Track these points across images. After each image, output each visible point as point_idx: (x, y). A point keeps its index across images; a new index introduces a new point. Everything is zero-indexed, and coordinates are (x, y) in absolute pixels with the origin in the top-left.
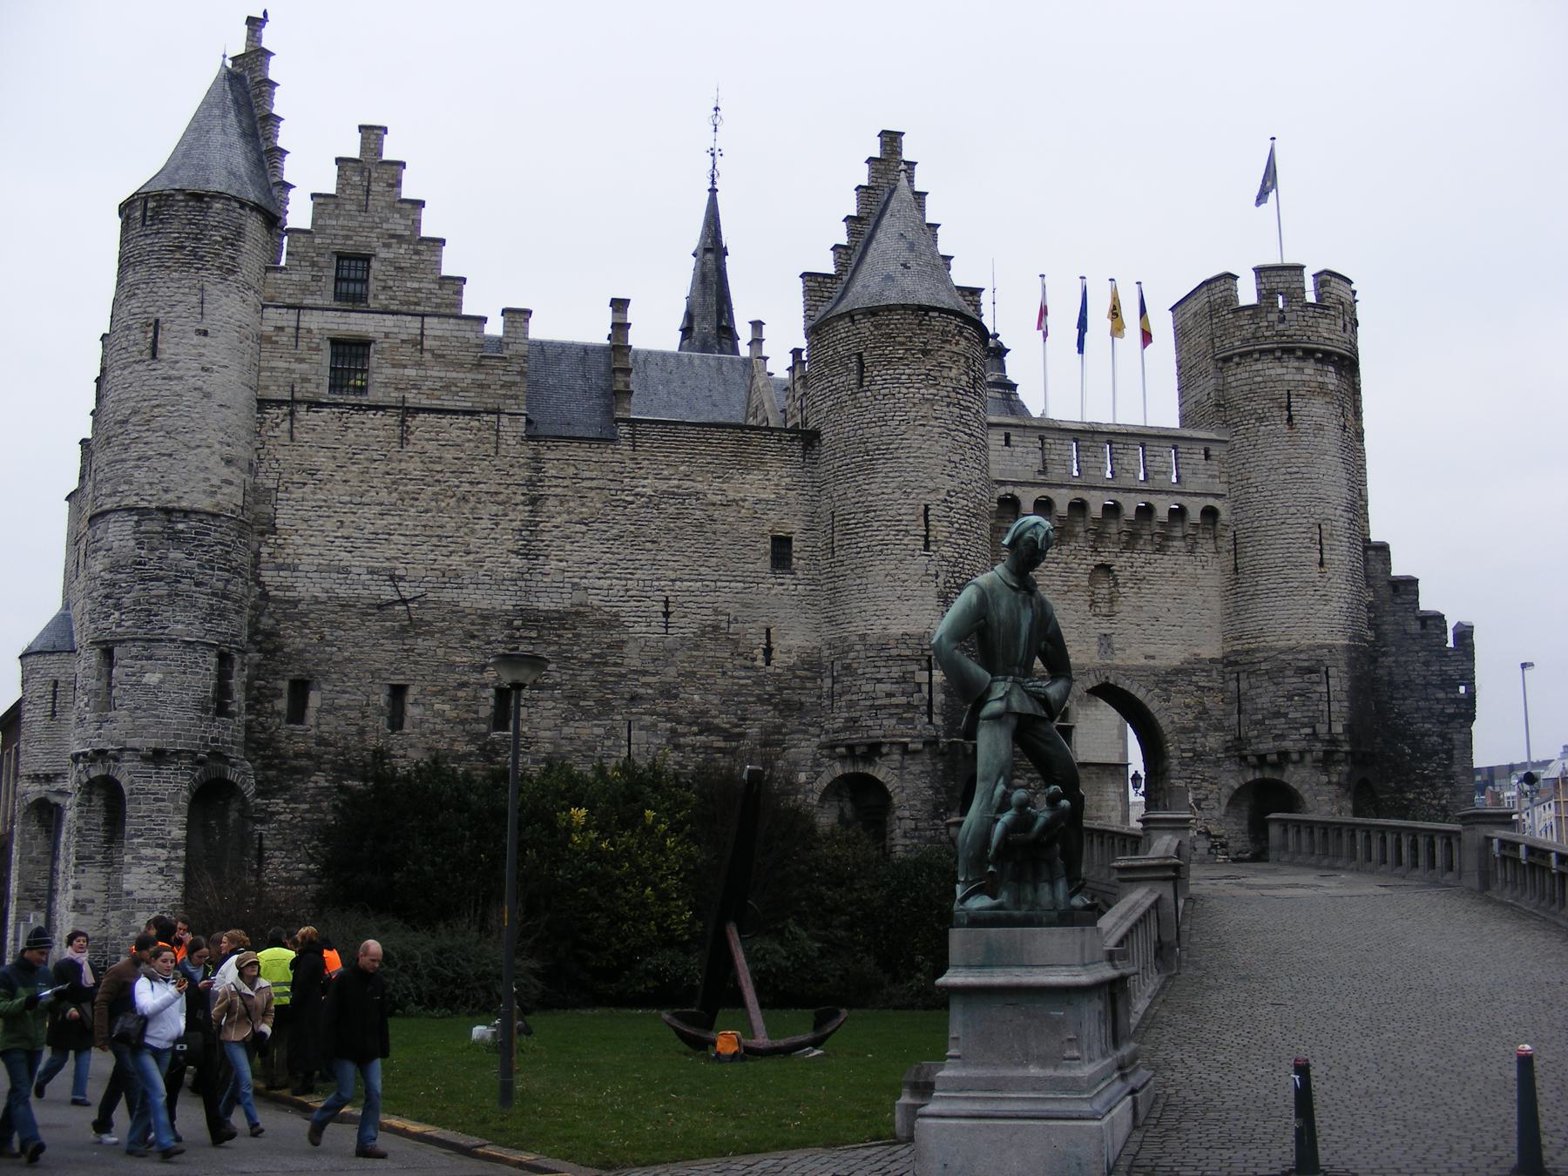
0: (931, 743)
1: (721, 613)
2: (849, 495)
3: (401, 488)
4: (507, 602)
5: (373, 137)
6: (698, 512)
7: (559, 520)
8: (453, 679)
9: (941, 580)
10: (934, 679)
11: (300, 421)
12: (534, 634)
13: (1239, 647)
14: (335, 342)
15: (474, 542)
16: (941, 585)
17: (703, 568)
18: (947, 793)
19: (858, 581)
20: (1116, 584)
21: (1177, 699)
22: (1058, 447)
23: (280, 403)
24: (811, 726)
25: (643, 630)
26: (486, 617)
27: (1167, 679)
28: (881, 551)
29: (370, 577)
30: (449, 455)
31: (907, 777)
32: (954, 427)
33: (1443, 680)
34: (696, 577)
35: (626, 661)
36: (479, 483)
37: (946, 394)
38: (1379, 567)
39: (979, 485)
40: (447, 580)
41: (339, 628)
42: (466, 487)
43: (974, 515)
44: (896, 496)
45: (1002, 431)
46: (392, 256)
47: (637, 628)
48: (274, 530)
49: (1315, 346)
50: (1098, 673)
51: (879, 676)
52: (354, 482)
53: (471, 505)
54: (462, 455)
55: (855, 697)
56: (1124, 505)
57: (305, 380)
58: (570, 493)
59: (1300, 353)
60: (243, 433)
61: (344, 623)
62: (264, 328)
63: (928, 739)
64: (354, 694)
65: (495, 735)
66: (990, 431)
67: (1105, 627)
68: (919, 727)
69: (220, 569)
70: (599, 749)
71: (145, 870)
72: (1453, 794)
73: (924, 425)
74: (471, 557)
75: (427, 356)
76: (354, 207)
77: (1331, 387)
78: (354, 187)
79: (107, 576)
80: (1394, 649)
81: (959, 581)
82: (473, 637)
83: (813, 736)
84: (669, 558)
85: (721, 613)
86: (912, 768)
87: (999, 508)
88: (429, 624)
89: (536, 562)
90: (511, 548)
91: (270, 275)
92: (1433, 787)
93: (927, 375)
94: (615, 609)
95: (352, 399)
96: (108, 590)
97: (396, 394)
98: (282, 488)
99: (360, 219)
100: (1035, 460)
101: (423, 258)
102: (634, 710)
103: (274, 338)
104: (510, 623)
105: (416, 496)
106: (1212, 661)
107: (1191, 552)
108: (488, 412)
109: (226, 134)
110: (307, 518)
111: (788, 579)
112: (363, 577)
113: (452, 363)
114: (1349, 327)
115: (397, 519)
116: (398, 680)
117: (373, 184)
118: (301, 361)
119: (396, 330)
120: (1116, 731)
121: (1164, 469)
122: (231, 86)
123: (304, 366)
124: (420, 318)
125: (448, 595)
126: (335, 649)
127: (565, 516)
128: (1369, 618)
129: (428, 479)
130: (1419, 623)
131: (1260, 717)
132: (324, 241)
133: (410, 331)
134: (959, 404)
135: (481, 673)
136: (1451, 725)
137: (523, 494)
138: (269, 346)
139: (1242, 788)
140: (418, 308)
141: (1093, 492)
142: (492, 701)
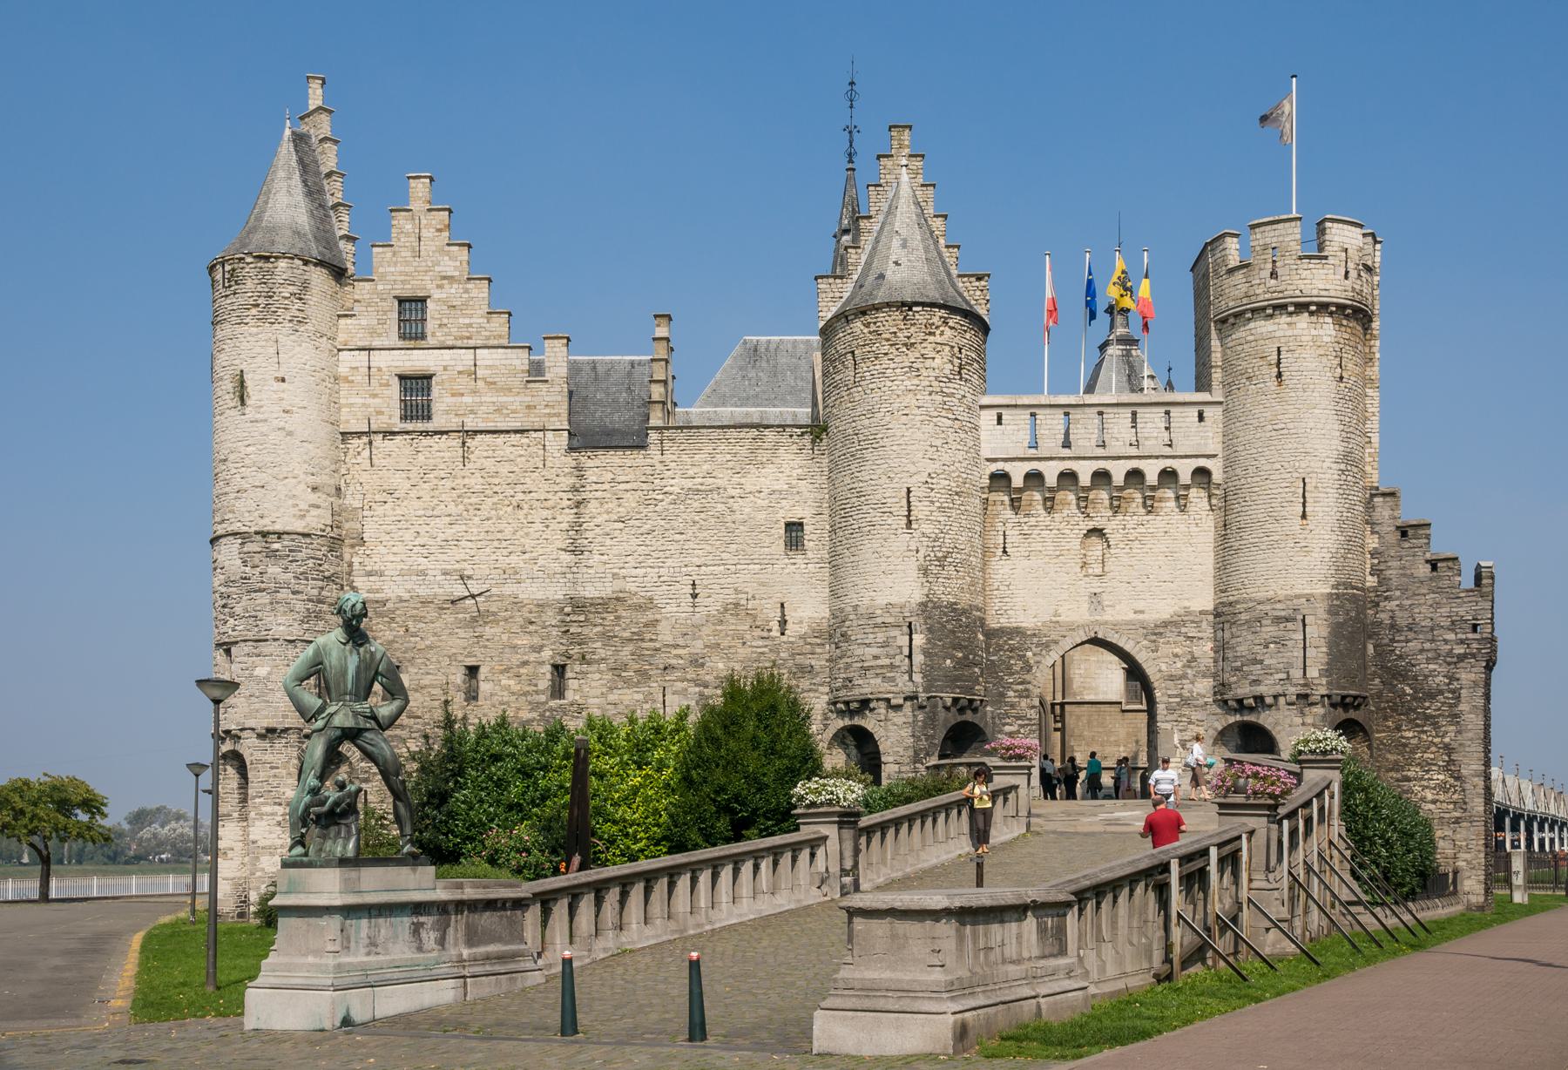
0: (911, 698)
1: (741, 592)
2: (846, 482)
3: (466, 500)
4: (561, 593)
5: (421, 186)
6: (719, 505)
7: (600, 520)
8: (516, 659)
9: (921, 555)
10: (914, 642)
11: (378, 448)
12: (582, 618)
13: (1225, 600)
14: (402, 378)
15: (528, 543)
16: (922, 559)
17: (725, 554)
18: (926, 740)
19: (852, 559)
20: (1109, 546)
21: (1165, 650)
22: (1049, 422)
23: (359, 434)
24: (822, 685)
25: (674, 610)
26: (541, 606)
27: (1157, 631)
28: (869, 531)
29: (444, 577)
30: (504, 469)
31: (891, 727)
33: (1453, 622)
34: (718, 562)
35: (660, 638)
36: (530, 492)
38: (1387, 513)
39: (964, 465)
40: (506, 576)
41: (420, 621)
42: (520, 496)
43: (957, 494)
44: (880, 482)
45: (994, 412)
46: (445, 295)
47: (669, 608)
48: (362, 541)
50: (1087, 629)
51: (867, 642)
52: (427, 498)
53: (525, 511)
54: (515, 469)
55: (849, 660)
56: (1113, 472)
57: (379, 413)
58: (609, 496)
60: (327, 463)
61: (425, 617)
62: (340, 370)
63: (909, 694)
64: (436, 675)
65: (554, 703)
67: (1096, 586)
68: (900, 685)
69: (314, 579)
70: (639, 711)
71: (266, 823)
72: (1459, 732)
74: (527, 556)
75: (480, 384)
76: (409, 254)
78: (408, 234)
79: (223, 589)
80: (1398, 593)
81: (940, 554)
82: (532, 623)
83: (822, 693)
84: (696, 546)
85: (741, 592)
86: (895, 720)
87: (990, 483)
88: (494, 614)
89: (581, 557)
90: (559, 547)
91: (342, 321)
92: (1436, 726)
94: (649, 594)
95: (420, 426)
96: (224, 601)
97: (457, 420)
98: (366, 507)
99: (415, 264)
100: (1025, 437)
101: (471, 295)
102: (667, 678)
103: (350, 378)
104: (563, 609)
105: (478, 506)
106: (1201, 613)
107: (1183, 509)
108: (535, 431)
109: (291, 195)
110: (389, 531)
111: (799, 559)
112: (438, 578)
113: (502, 389)
115: (464, 528)
116: (471, 662)
117: (423, 230)
118: (375, 396)
119: (453, 363)
122: (296, 146)
123: (377, 401)
124: (472, 351)
125: (508, 589)
126: (419, 639)
127: (605, 517)
128: (1373, 565)
129: (487, 492)
130: (1429, 566)
131: (1239, 664)
132: (386, 287)
133: (464, 362)
135: (539, 652)
136: (1461, 664)
137: (569, 499)
138: (347, 385)
139: (1225, 728)
140: (470, 341)
141: (1081, 462)
142: (549, 676)
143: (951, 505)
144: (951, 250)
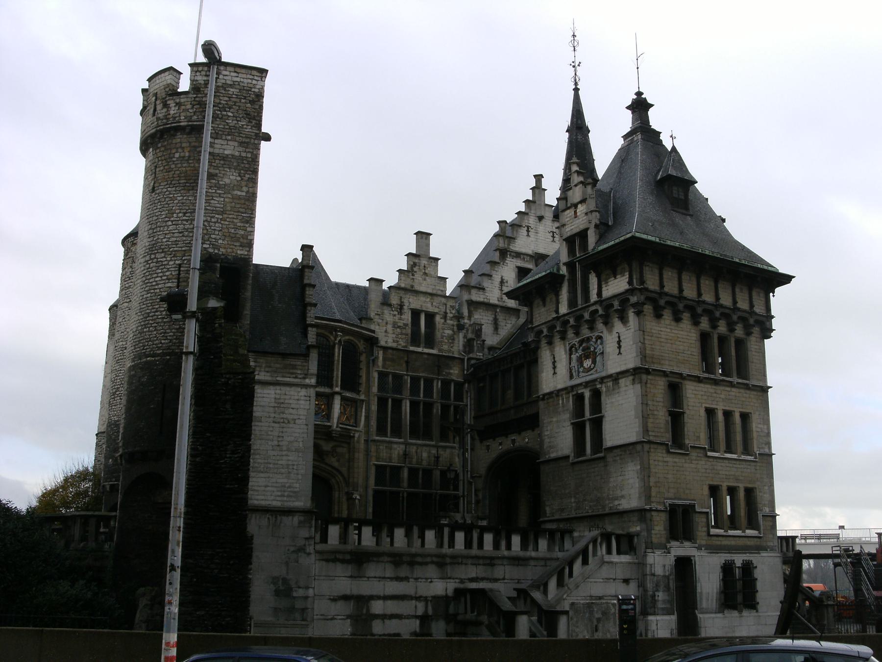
120: (633, 413)
143: (122, 357)
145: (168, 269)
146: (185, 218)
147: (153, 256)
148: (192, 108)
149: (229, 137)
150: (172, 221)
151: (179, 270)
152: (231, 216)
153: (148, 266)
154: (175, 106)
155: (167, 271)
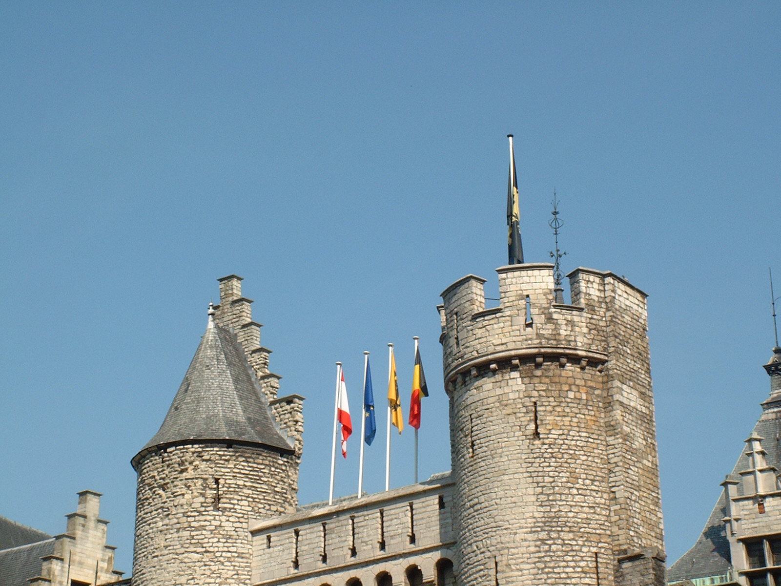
32: (183, 550)
37: (176, 521)
49: (484, 359)
59: (474, 372)
66: (255, 538)
73: (157, 556)
77: (511, 396)
93: (162, 508)
114: (539, 320)
121: (400, 531)
134: (190, 527)
144: (266, 380)
145: (582, 557)
146: (593, 487)
147: (554, 535)
148: (589, 333)
149: (631, 383)
150: (578, 489)
151: (597, 562)
152: (645, 494)
153: (546, 547)
154: (566, 325)
155: (580, 561)
